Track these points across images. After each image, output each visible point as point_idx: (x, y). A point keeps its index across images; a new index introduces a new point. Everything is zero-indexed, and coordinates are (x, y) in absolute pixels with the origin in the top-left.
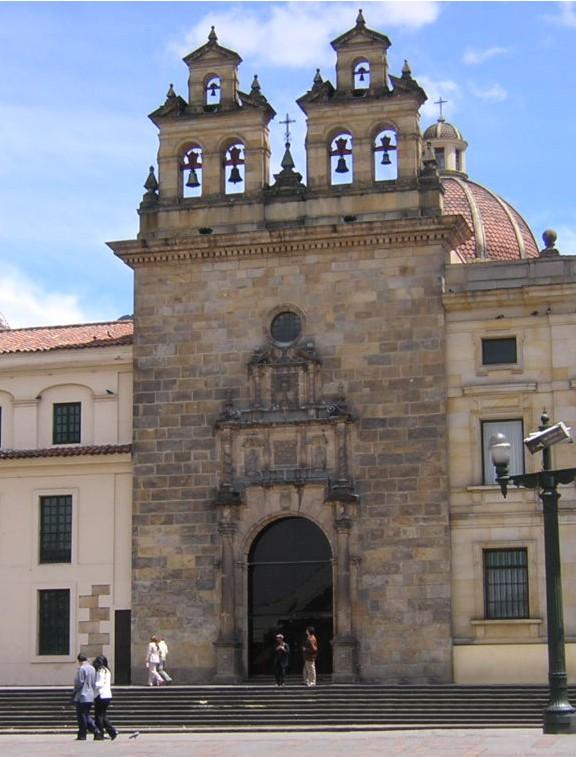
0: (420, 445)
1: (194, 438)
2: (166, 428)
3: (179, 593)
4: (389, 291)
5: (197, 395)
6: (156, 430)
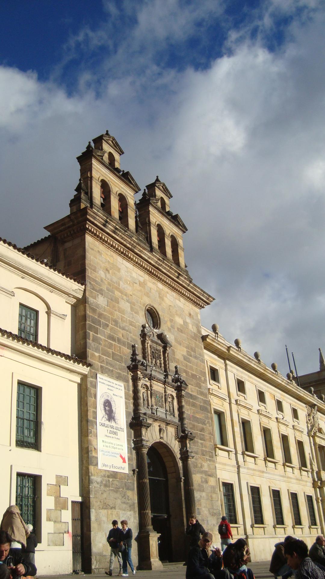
0: (203, 415)
1: (119, 371)
2: (105, 357)
3: (116, 491)
4: (187, 322)
5: (119, 341)
6: (100, 356)
